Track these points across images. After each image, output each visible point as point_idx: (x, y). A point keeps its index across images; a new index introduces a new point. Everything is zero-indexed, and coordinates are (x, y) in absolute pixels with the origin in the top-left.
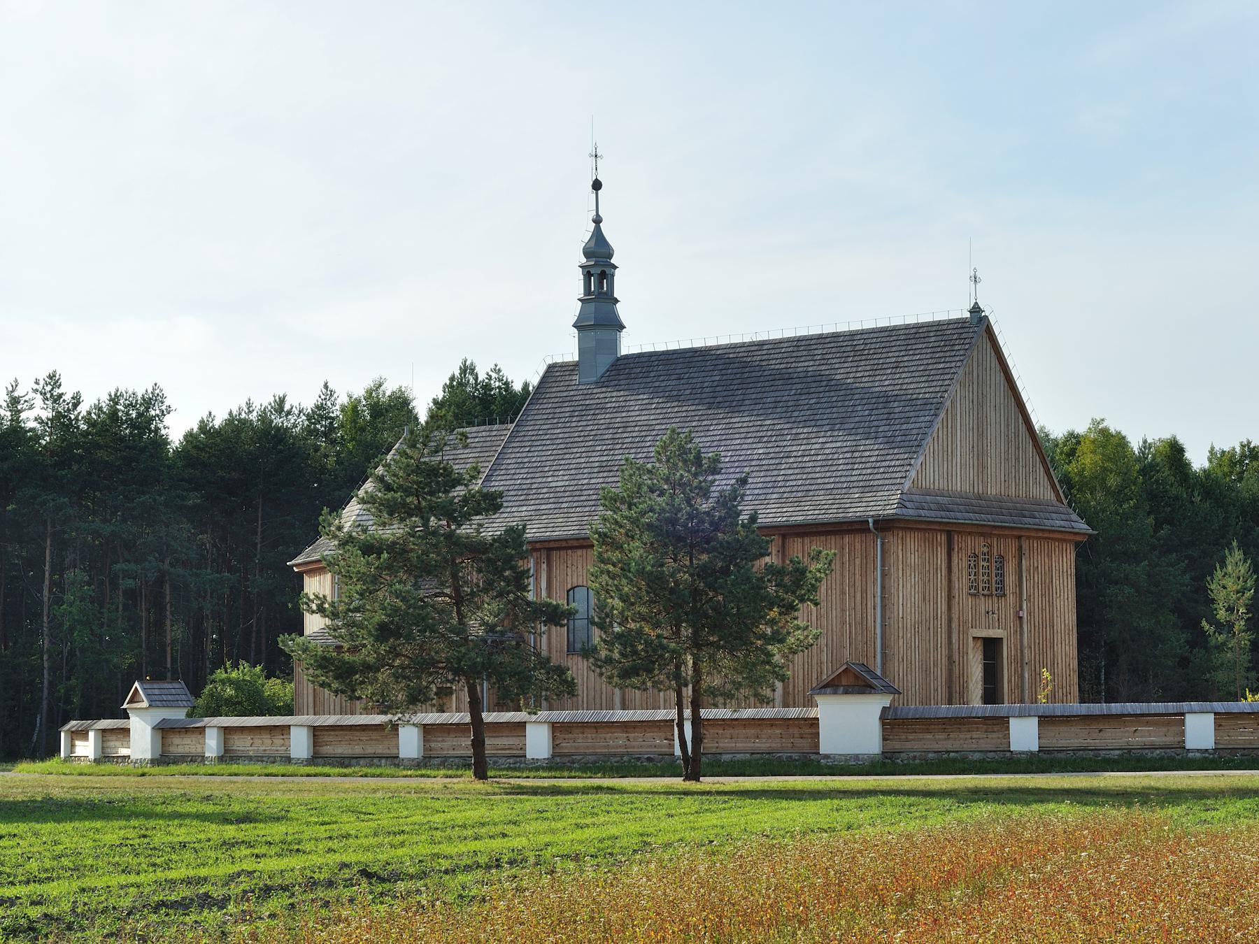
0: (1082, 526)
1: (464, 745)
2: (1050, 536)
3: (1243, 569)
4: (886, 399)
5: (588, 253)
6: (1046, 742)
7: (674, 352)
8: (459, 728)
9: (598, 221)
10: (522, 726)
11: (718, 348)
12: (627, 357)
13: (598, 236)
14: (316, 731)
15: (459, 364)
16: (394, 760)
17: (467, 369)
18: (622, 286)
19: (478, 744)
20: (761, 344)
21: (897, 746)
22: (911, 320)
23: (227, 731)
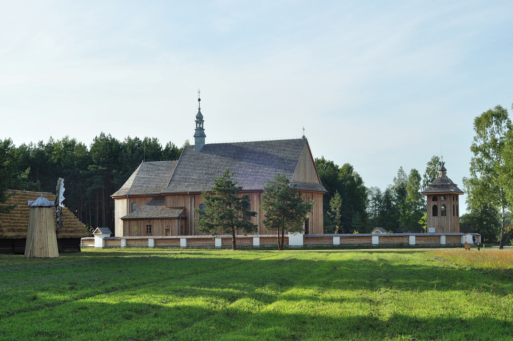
0: (325, 190)
1: (231, 242)
2: (318, 192)
3: (339, 198)
5: (197, 118)
7: (221, 144)
8: (230, 239)
9: (199, 109)
10: (179, 239)
11: (234, 143)
13: (199, 113)
14: (155, 240)
15: (100, 133)
16: (179, 247)
17: (102, 135)
18: (205, 126)
19: (234, 242)
20: (246, 143)
21: (307, 243)
23: (127, 240)
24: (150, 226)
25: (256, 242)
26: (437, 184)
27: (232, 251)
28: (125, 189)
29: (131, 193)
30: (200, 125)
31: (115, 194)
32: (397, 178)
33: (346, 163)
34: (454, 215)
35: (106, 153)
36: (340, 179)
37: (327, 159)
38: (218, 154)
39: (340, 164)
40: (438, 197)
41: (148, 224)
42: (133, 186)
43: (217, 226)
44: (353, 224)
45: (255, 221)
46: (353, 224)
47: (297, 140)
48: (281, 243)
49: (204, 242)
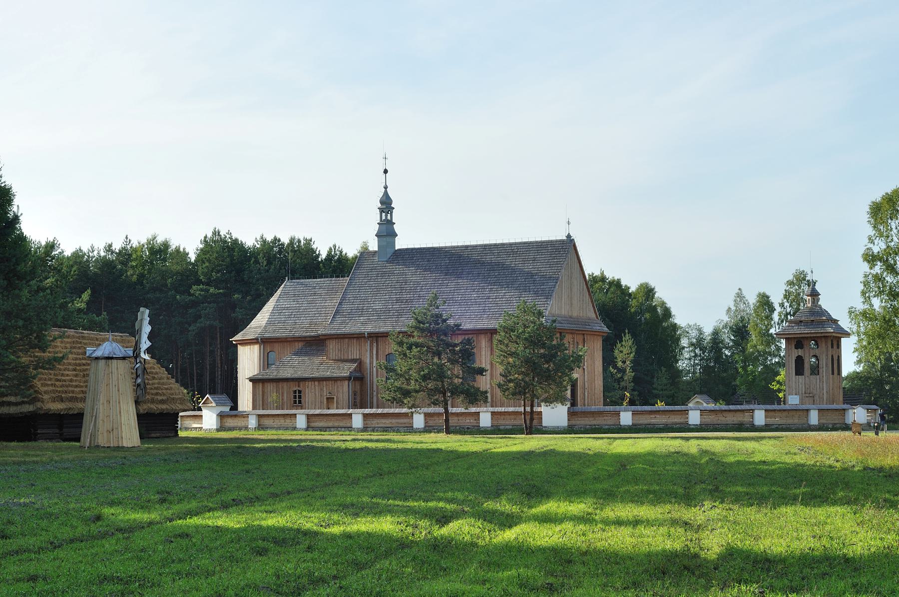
0: (606, 329)
1: (441, 421)
2: (594, 333)
3: (630, 343)
4: (531, 275)
5: (382, 202)
6: (635, 422)
7: (424, 248)
8: (439, 414)
9: (386, 188)
10: (350, 415)
11: (446, 247)
12: (400, 250)
14: (309, 417)
15: (212, 230)
16: (350, 428)
17: (216, 233)
19: (447, 421)
20: (467, 247)
21: (573, 422)
22: (539, 239)
23: (260, 416)
24: (300, 392)
25: (485, 420)
26: (803, 319)
27: (442, 436)
28: (256, 328)
29: (267, 335)
30: (386, 216)
31: (238, 337)
32: (733, 308)
33: (643, 281)
34: (833, 373)
35: (221, 265)
36: (633, 310)
37: (610, 275)
38: (418, 267)
39: (632, 283)
40: (805, 343)
41: (296, 388)
42: (269, 323)
43: (417, 391)
44: (655, 389)
45: (484, 383)
46: (655, 389)
47: (557, 241)
48: (528, 422)
49: (394, 421)
